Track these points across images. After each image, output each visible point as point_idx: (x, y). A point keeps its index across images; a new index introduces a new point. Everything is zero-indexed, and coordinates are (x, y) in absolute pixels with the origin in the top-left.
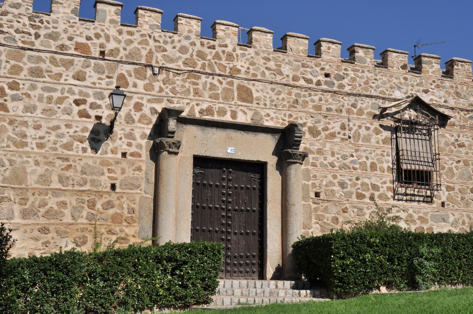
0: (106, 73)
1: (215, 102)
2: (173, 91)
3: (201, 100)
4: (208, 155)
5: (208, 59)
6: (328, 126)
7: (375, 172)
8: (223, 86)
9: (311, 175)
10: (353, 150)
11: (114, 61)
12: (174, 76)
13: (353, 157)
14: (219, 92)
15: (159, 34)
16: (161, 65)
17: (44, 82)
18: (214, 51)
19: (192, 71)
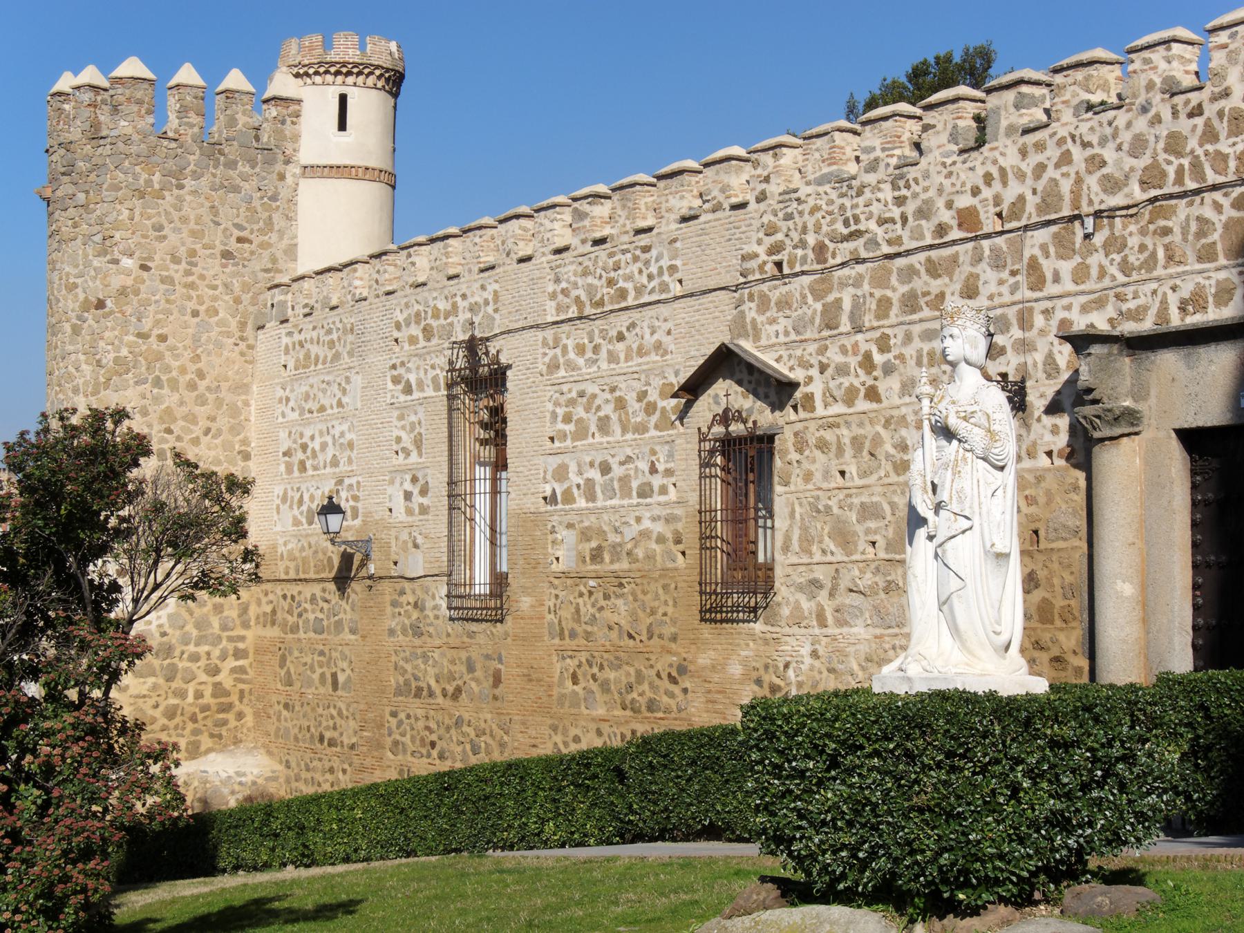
0: (1009, 267)
1: (1208, 271)
2: (1125, 268)
3: (1179, 275)
4: (1201, 424)
5: (1188, 149)
8: (1224, 218)
11: (1019, 229)
12: (1125, 227)
14: (1216, 236)
15: (1089, 124)
16: (1097, 207)
17: (921, 321)
18: (1199, 121)
19: (1156, 199)
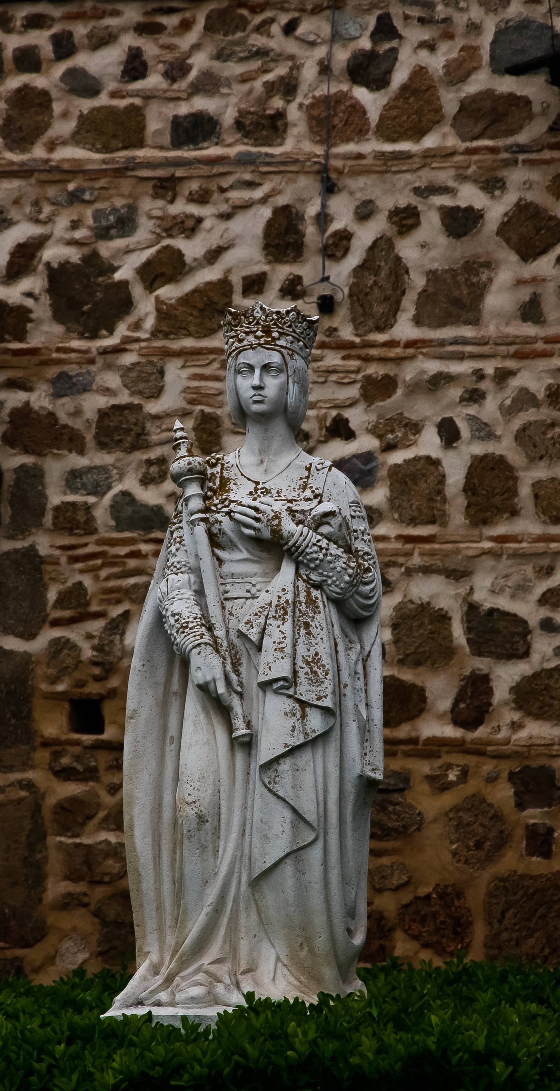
6: (180, 243)
7: (501, 529)
9: (52, 595)
10: (354, 392)
13: (349, 435)
